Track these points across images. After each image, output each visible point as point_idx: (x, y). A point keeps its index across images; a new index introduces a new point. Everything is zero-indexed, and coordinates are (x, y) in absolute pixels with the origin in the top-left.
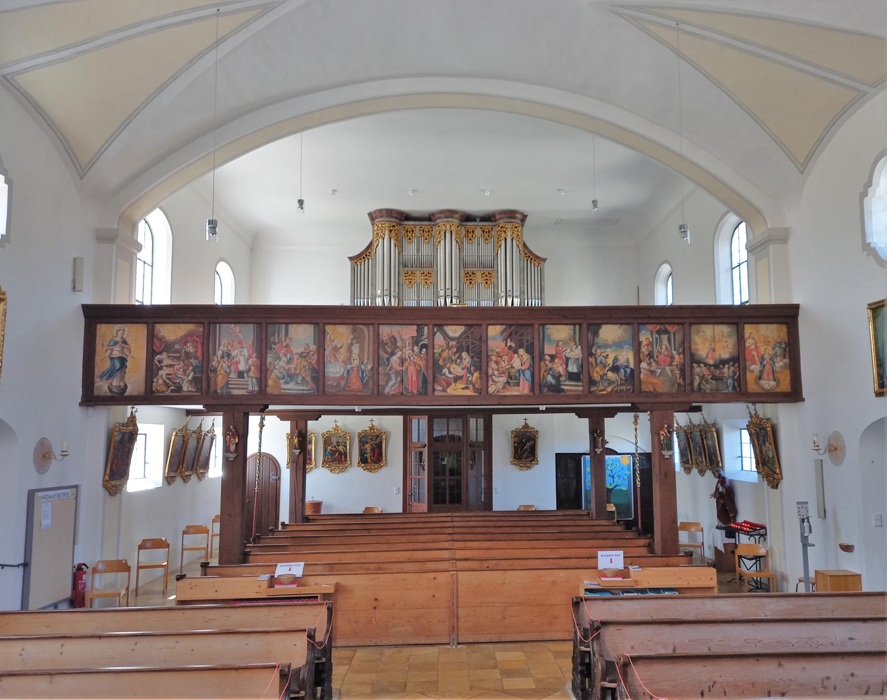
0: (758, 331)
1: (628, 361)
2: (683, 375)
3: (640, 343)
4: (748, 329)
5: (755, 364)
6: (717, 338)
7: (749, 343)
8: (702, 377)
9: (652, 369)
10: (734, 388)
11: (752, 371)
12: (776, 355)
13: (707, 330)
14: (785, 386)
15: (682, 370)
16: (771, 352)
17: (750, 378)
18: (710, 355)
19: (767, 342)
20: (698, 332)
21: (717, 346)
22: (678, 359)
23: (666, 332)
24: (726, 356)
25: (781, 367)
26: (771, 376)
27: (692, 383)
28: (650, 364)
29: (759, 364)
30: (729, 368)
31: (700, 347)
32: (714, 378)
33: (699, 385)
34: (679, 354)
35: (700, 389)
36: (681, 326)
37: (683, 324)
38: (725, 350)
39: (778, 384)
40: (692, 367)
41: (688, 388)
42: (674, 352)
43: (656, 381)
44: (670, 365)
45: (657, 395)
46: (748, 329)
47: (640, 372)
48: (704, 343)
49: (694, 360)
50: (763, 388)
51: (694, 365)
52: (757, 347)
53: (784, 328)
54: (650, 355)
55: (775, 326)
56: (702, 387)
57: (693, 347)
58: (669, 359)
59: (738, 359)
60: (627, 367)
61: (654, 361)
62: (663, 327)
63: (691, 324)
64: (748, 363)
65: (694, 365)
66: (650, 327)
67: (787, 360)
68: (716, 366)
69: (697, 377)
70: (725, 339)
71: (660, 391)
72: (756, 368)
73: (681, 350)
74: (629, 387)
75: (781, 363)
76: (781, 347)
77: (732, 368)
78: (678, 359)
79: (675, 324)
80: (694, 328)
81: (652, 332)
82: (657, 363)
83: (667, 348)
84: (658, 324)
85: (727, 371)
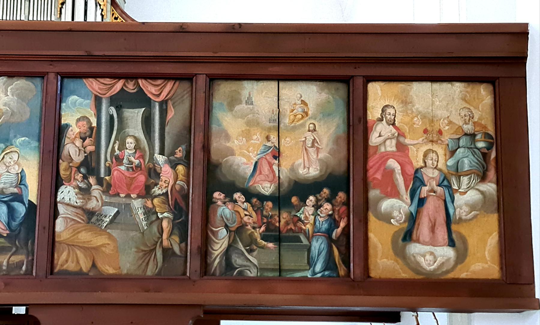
0: (406, 102)
1: (21, 181)
2: (181, 227)
3: (61, 131)
4: (380, 96)
5: (396, 194)
6: (286, 121)
7: (380, 136)
8: (238, 232)
9: (93, 204)
10: (330, 264)
11: (386, 218)
12: (458, 172)
13: (260, 96)
14: (484, 262)
15: (179, 207)
16: (444, 162)
17: (380, 236)
18: (265, 169)
19: (432, 134)
20: (233, 101)
21: (286, 143)
22: (169, 177)
23: (141, 100)
24: (311, 171)
25: (472, 207)
26: (442, 233)
27: (204, 252)
28: (85, 192)
29: (406, 197)
30: (317, 206)
31: (235, 143)
32: (275, 235)
33: (227, 254)
34: (174, 166)
35: (229, 265)
36: (186, 85)
37: (189, 78)
38: (310, 154)
39: (461, 257)
40: (208, 203)
41: (193, 265)
42: (160, 159)
43: (99, 241)
44: (146, 192)
45: (96, 280)
46: (380, 96)
47: (55, 214)
48: (247, 135)
49: (212, 178)
50: (416, 268)
51: (217, 195)
52: (401, 147)
53: (484, 95)
54: (90, 166)
55: (458, 87)
56: (237, 261)
57: (216, 144)
58: (142, 178)
59: (349, 181)
60: (18, 198)
61: (100, 181)
62: (131, 87)
63: (213, 79)
64: (374, 193)
65: (217, 195)
66: (94, 85)
67: (490, 187)
68: (280, 200)
69: (223, 232)
70: (308, 123)
71: (109, 270)
72: (397, 207)
73: (179, 153)
74: (16, 259)
75: (473, 196)
76: (472, 148)
77: (327, 206)
78: (169, 177)
79: (167, 77)
80: (224, 89)
81: (98, 100)
82: (107, 188)
83: (138, 147)
84: (117, 77)
85: (312, 215)
